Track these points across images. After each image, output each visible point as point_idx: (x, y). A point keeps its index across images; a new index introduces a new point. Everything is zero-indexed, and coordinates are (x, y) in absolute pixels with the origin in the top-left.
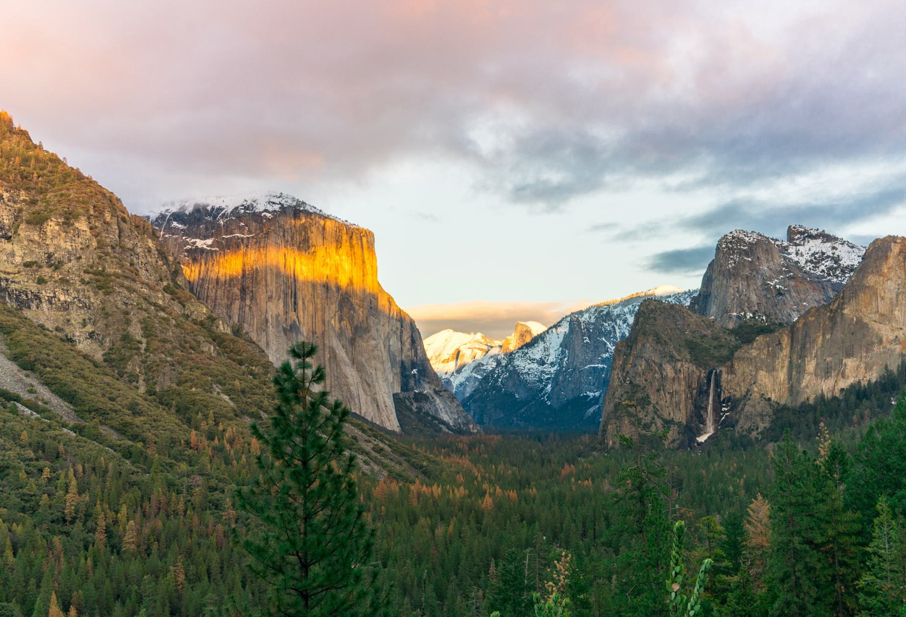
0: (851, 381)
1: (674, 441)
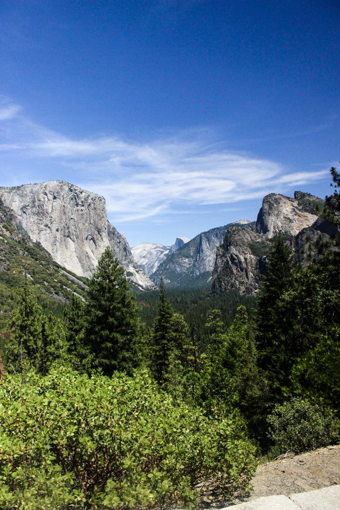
1: (244, 292)
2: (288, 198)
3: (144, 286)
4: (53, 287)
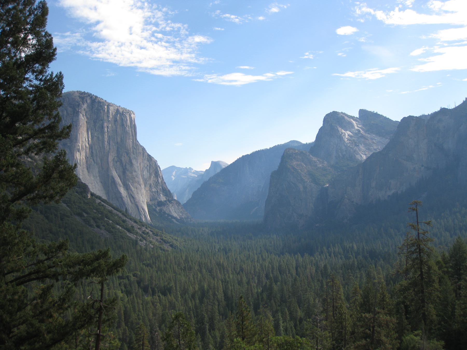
0: (393, 191)
2: (353, 118)
3: (178, 218)
4: (93, 219)
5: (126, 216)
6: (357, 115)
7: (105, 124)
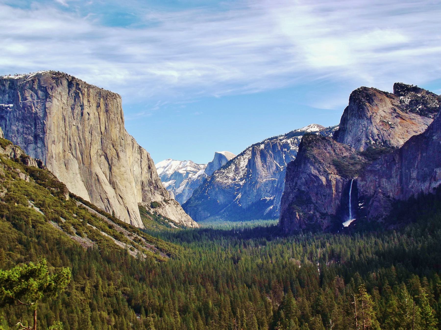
2: (386, 94)
3: (177, 221)
4: (73, 225)
5: (113, 220)
6: (391, 90)
7: (86, 111)
